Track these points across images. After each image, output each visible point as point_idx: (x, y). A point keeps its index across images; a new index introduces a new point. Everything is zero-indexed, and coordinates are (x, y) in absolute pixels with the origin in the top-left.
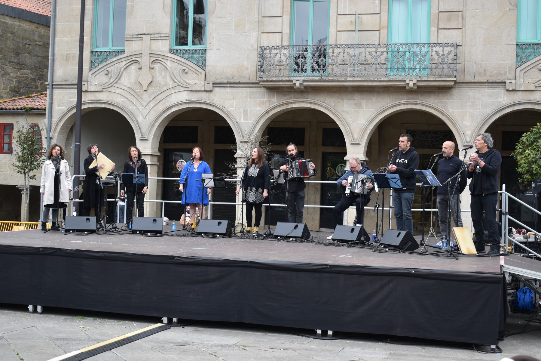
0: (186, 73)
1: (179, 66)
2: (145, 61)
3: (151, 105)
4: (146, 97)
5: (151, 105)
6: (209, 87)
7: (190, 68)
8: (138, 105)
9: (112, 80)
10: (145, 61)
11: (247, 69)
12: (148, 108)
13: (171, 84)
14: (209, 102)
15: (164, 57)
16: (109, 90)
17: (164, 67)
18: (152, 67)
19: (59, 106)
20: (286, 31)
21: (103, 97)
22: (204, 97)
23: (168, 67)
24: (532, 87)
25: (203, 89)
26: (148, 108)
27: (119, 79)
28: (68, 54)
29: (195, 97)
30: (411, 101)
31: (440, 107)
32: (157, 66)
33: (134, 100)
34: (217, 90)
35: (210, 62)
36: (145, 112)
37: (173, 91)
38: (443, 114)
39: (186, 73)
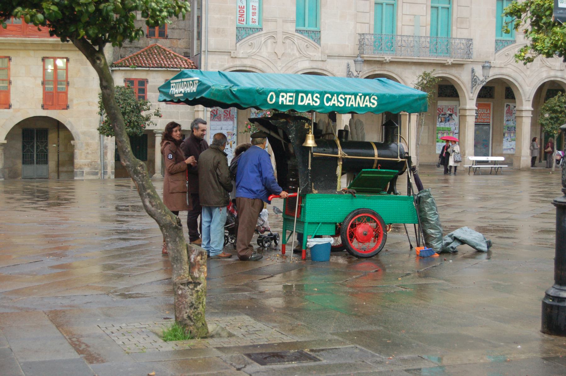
0: (308, 47)
1: (303, 43)
2: (280, 38)
7: (311, 44)
10: (280, 38)
11: (348, 47)
13: (297, 54)
14: (325, 68)
15: (292, 35)
16: (253, 57)
17: (292, 42)
18: (284, 42)
19: (212, 68)
20: (372, 23)
23: (296, 43)
24: (502, 66)
25: (320, 59)
27: (260, 49)
28: (218, 28)
30: (444, 72)
31: (457, 75)
32: (288, 41)
33: (271, 65)
34: (329, 60)
35: (323, 41)
37: (299, 60)
38: (459, 79)
39: (308, 47)
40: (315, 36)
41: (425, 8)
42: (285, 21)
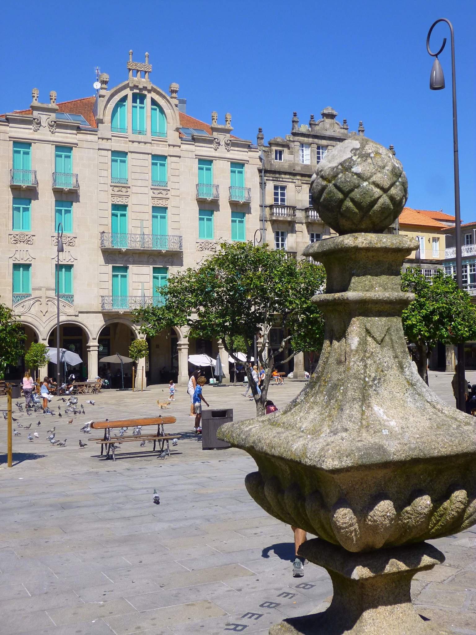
2: (44, 300)
3: (47, 322)
4: (44, 319)
5: (47, 322)
6: (77, 314)
8: (41, 322)
9: (25, 310)
10: (44, 300)
12: (46, 323)
21: (22, 318)
22: (74, 318)
26: (46, 323)
29: (70, 318)
32: (49, 303)
35: (75, 303)
36: (44, 325)
40: (70, 298)
41: (148, 277)
42: (48, 289)
